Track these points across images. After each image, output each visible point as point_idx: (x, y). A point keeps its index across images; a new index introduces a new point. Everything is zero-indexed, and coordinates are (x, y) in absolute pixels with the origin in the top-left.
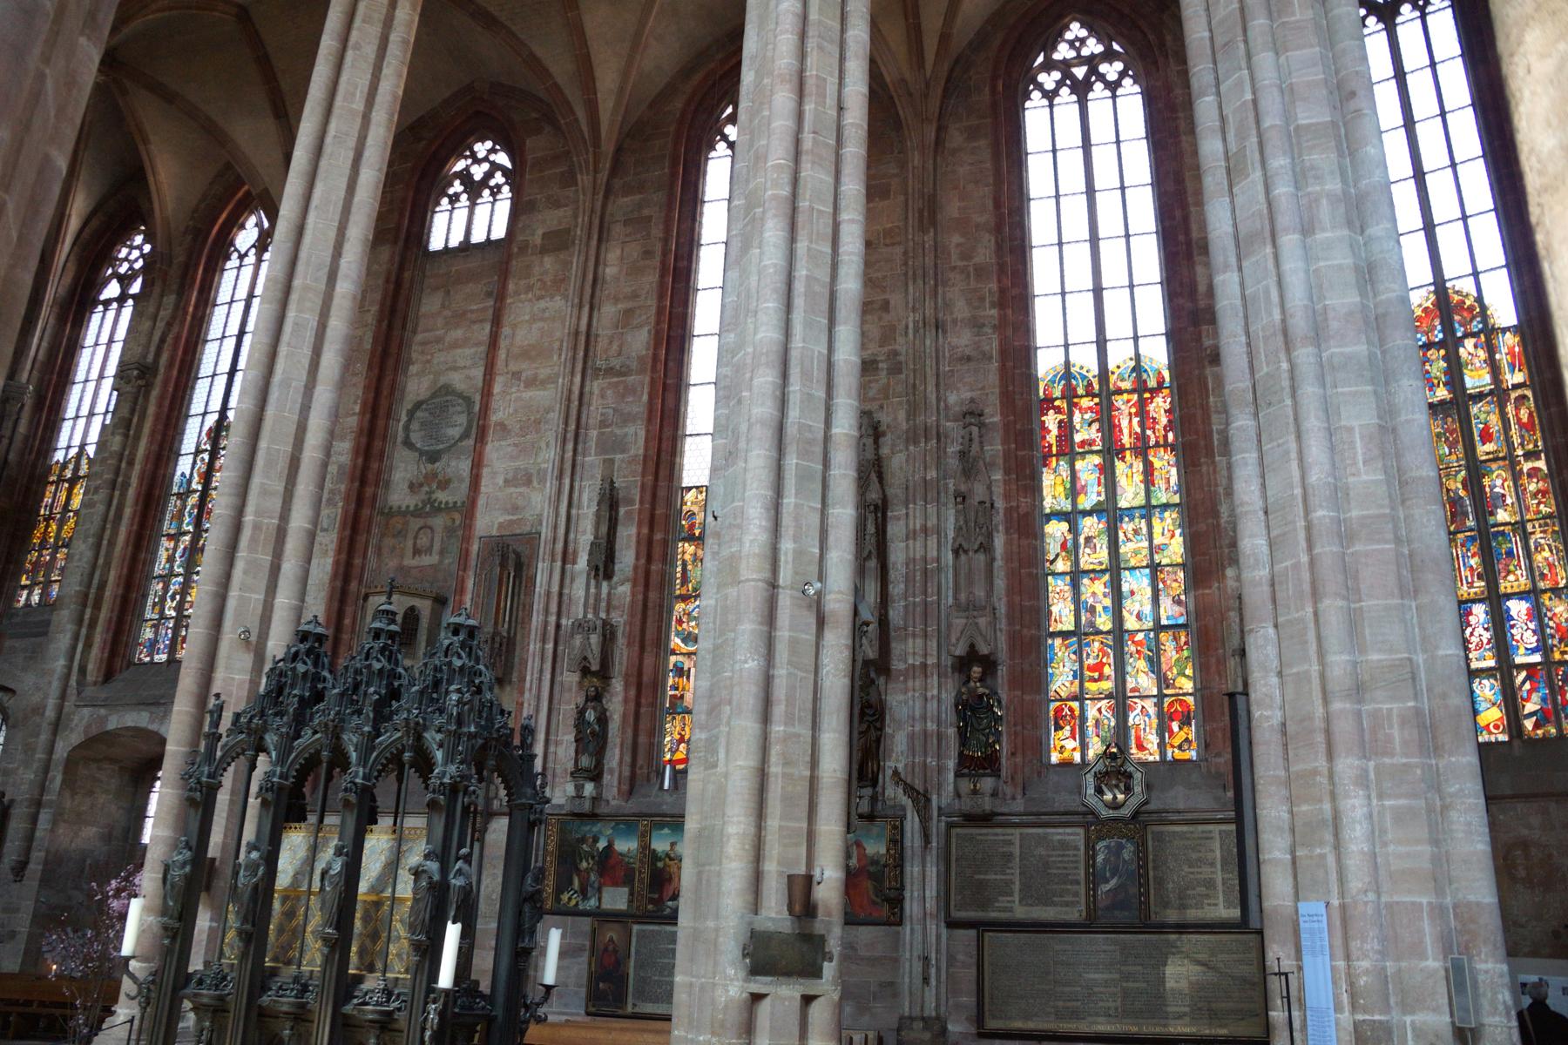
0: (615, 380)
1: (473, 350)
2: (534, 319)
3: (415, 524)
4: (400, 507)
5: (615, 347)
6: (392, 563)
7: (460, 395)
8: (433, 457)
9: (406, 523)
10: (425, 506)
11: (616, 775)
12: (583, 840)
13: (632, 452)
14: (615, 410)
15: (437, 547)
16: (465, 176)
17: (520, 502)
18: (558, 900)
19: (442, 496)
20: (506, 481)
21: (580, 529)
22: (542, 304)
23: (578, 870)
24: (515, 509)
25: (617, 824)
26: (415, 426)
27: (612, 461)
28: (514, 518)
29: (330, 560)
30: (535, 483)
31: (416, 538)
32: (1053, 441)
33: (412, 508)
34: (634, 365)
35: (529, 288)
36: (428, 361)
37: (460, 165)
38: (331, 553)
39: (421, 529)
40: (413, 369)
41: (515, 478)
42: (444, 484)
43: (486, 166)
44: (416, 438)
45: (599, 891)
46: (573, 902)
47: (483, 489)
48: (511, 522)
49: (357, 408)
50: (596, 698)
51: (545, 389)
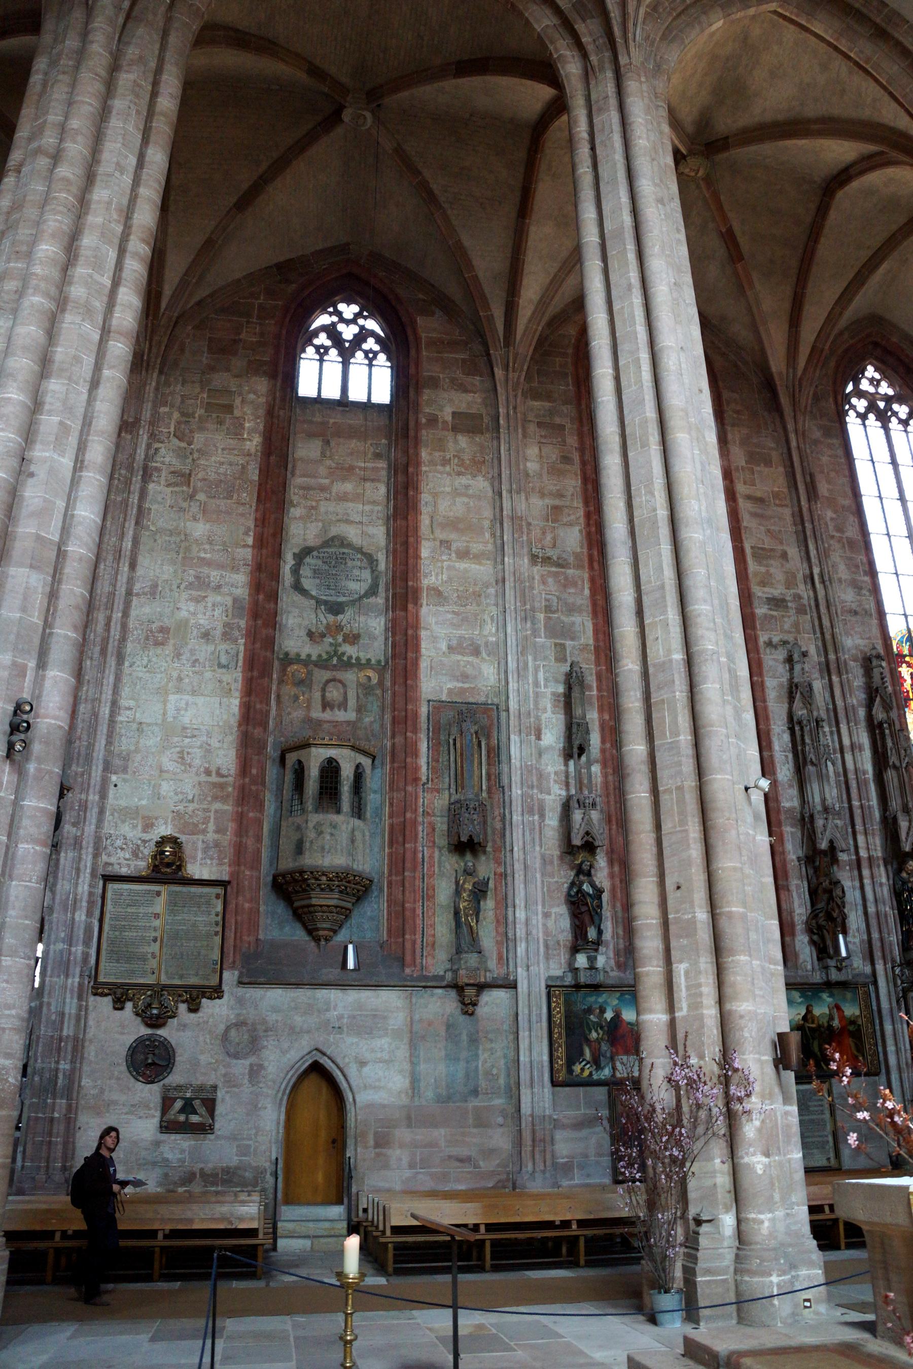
0: (554, 569)
1: (367, 508)
2: (456, 493)
3: (322, 676)
4: (298, 655)
5: (549, 537)
6: (298, 714)
7: (360, 550)
8: (336, 609)
9: (310, 673)
10: (331, 657)
11: (611, 947)
12: (589, 1011)
13: (582, 641)
14: (558, 598)
15: (352, 703)
16: (331, 331)
17: (469, 670)
18: (570, 1071)
19: (350, 650)
20: (450, 648)
21: (540, 706)
22: (464, 480)
23: (588, 1041)
24: (465, 677)
25: (622, 995)
26: (305, 571)
27: (563, 646)
28: (466, 686)
29: (237, 702)
30: (484, 655)
31: (323, 690)
32: (909, 688)
33: (314, 658)
34: (571, 559)
35: (445, 462)
36: (313, 508)
37: (324, 319)
38: (237, 694)
39: (328, 682)
40: (295, 512)
41: (460, 645)
42: (353, 639)
43: (354, 329)
44: (307, 583)
45: (612, 1059)
46: (586, 1073)
47: (423, 651)
48: (462, 691)
49: (250, 541)
50: (584, 872)
51: (480, 564)
